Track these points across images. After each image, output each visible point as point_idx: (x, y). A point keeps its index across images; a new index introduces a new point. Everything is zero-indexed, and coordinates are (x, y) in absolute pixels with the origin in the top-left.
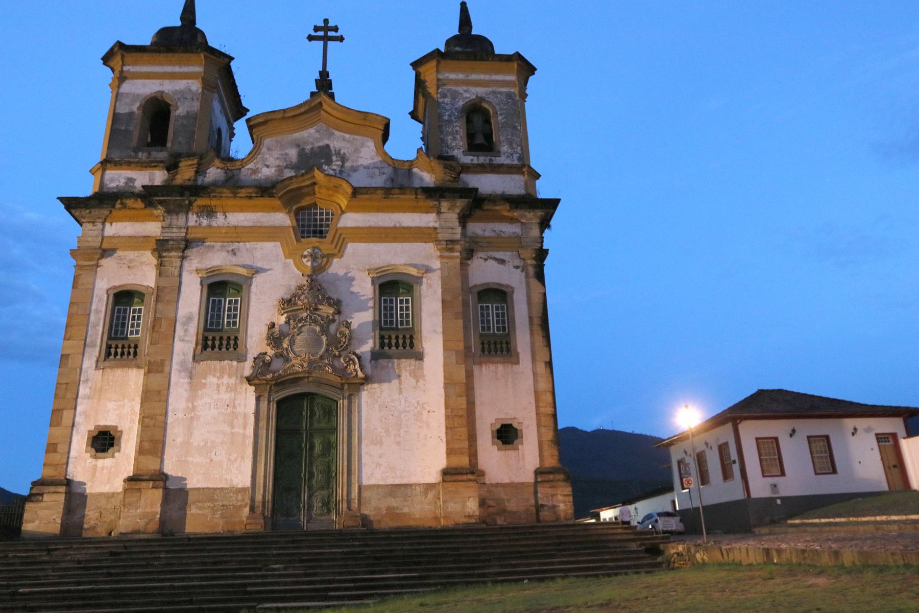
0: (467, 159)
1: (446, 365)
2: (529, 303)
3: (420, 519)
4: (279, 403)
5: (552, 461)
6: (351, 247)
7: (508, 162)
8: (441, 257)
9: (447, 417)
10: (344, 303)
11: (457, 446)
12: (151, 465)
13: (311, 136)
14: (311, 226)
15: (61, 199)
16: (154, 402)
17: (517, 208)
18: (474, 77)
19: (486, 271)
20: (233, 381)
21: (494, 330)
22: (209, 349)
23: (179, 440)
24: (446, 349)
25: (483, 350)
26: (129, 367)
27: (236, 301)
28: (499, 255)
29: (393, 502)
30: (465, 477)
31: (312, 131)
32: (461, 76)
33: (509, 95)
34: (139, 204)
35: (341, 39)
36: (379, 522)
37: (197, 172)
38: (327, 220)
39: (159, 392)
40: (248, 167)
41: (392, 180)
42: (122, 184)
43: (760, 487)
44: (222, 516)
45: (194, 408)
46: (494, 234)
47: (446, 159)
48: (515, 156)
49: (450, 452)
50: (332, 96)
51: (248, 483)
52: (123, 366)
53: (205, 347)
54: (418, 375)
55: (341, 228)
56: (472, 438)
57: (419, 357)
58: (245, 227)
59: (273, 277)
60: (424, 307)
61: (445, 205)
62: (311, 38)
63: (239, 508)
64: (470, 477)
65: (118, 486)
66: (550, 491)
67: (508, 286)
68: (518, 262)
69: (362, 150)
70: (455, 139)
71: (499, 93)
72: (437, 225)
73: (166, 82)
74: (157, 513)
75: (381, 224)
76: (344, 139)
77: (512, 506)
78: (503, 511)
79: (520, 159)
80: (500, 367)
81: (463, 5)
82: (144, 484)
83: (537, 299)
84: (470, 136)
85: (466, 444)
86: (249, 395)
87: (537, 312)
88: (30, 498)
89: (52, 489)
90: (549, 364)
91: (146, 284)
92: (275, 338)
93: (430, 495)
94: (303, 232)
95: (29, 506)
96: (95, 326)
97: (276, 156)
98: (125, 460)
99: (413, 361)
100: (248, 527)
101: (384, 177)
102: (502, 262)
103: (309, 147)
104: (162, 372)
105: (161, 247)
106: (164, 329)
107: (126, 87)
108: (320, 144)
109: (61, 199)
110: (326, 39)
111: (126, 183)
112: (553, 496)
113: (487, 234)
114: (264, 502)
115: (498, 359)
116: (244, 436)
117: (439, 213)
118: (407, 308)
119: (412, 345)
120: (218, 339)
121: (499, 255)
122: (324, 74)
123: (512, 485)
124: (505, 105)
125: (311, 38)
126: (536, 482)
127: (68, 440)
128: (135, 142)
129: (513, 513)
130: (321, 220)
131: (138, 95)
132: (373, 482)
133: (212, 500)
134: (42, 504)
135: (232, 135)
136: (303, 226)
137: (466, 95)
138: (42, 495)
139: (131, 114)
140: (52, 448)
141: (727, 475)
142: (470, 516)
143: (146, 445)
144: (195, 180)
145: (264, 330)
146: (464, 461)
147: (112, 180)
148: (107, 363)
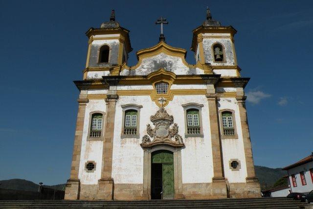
0: (213, 64)
3: (206, 196)
5: (253, 175)
7: (230, 65)
9: (213, 158)
11: (217, 169)
12: (107, 175)
15: (75, 82)
16: (108, 153)
19: (224, 105)
22: (126, 134)
24: (212, 133)
27: (135, 117)
30: (221, 181)
31: (159, 55)
33: (228, 41)
36: (190, 197)
39: (110, 149)
41: (188, 72)
42: (94, 77)
47: (208, 64)
49: (215, 171)
51: (142, 183)
53: (125, 133)
57: (202, 136)
59: (148, 107)
62: (156, 24)
64: (223, 180)
65: (96, 182)
67: (232, 110)
74: (110, 193)
76: (171, 58)
79: (234, 64)
80: (231, 140)
82: (106, 182)
84: (215, 56)
85: (221, 168)
86: (142, 151)
88: (67, 185)
89: (74, 182)
90: (250, 138)
92: (150, 130)
93: (208, 187)
94: (158, 91)
97: (148, 64)
100: (143, 198)
101: (186, 71)
102: (230, 101)
104: (110, 142)
105: (109, 98)
106: (110, 127)
108: (163, 60)
109: (75, 82)
112: (253, 187)
114: (148, 189)
115: (231, 137)
118: (197, 119)
120: (130, 131)
121: (229, 99)
127: (220, 160)
128: (97, 61)
130: (164, 87)
133: (129, 188)
134: (70, 188)
135: (128, 58)
136: (158, 89)
143: (106, 168)
144: (119, 74)
145: (146, 128)
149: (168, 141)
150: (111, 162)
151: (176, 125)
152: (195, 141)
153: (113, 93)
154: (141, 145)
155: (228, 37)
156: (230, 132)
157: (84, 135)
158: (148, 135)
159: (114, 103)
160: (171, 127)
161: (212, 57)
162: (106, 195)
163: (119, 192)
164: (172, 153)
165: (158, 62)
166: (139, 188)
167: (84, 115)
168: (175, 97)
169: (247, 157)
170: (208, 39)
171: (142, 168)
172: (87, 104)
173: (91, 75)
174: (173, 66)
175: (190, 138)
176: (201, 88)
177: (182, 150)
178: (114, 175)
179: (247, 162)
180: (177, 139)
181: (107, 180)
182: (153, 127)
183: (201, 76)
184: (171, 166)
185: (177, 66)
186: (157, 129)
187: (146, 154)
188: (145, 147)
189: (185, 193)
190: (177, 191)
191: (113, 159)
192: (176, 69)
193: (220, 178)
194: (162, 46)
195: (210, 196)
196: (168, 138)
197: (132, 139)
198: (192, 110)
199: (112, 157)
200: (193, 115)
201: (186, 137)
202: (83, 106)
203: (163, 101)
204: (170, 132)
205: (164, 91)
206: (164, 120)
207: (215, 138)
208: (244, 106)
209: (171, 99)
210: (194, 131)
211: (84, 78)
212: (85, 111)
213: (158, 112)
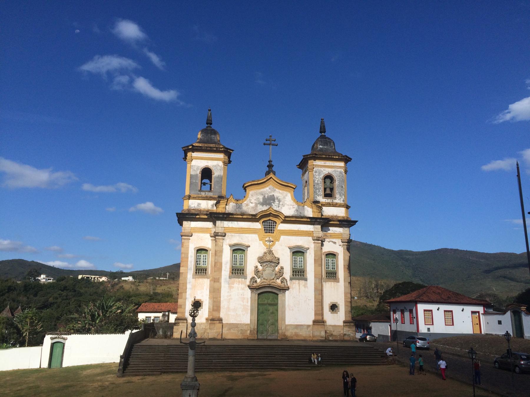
1: (315, 284)
4: (259, 294)
5: (349, 319)
12: (215, 315)
14: (269, 228)
19: (328, 247)
20: (243, 286)
21: (330, 269)
23: (226, 306)
24: (315, 277)
28: (334, 240)
29: (296, 330)
31: (267, 188)
33: (341, 173)
37: (226, 205)
40: (245, 202)
42: (196, 206)
44: (241, 333)
45: (230, 295)
46: (332, 232)
47: (316, 202)
48: (342, 199)
49: (316, 314)
51: (249, 322)
54: (305, 286)
57: (306, 280)
59: (256, 248)
62: (264, 144)
63: (246, 331)
64: (322, 323)
70: (319, 191)
71: (337, 171)
73: (209, 161)
76: (279, 193)
77: (334, 333)
78: (332, 335)
79: (343, 201)
80: (332, 283)
81: (322, 123)
82: (215, 322)
84: (325, 189)
89: (182, 321)
91: (208, 246)
92: (257, 272)
94: (265, 230)
95: (175, 327)
96: (191, 262)
101: (294, 209)
102: (335, 243)
103: (266, 196)
105: (215, 235)
106: (218, 266)
107: (194, 163)
120: (238, 271)
121: (334, 240)
123: (335, 326)
126: (344, 326)
129: (335, 336)
131: (198, 167)
132: (290, 323)
133: (237, 327)
137: (324, 172)
139: (197, 175)
141: (412, 323)
143: (215, 308)
145: (253, 269)
146: (320, 318)
147: (192, 204)
148: (196, 276)
149: (274, 284)
150: (220, 302)
151: (282, 268)
152: (299, 283)
153: (220, 230)
154: (249, 286)
155: (340, 167)
156: (332, 275)
157: (189, 271)
159: (221, 241)
160: (277, 269)
161: (322, 192)
162: (216, 335)
163: (227, 332)
164: (278, 295)
166: (245, 328)
167: (188, 250)
168: (282, 238)
169: (346, 301)
170: (320, 169)
171: (250, 308)
172: (190, 238)
173: (193, 204)
174: (281, 203)
178: (222, 315)
179: (345, 305)
180: (282, 282)
181: (215, 320)
182: (260, 268)
183: (310, 218)
184: (276, 307)
185: (286, 202)
186: (264, 270)
189: (288, 334)
190: (280, 331)
191: (222, 299)
193: (319, 322)
194: (271, 177)
195: (310, 337)
196: (274, 280)
200: (299, 258)
201: (291, 279)
202: (186, 241)
203: (270, 241)
204: (276, 275)
205: (271, 230)
206: (271, 262)
208: (348, 249)
209: (278, 240)
210: (299, 273)
211: (185, 207)
212: (189, 246)
213: (265, 253)
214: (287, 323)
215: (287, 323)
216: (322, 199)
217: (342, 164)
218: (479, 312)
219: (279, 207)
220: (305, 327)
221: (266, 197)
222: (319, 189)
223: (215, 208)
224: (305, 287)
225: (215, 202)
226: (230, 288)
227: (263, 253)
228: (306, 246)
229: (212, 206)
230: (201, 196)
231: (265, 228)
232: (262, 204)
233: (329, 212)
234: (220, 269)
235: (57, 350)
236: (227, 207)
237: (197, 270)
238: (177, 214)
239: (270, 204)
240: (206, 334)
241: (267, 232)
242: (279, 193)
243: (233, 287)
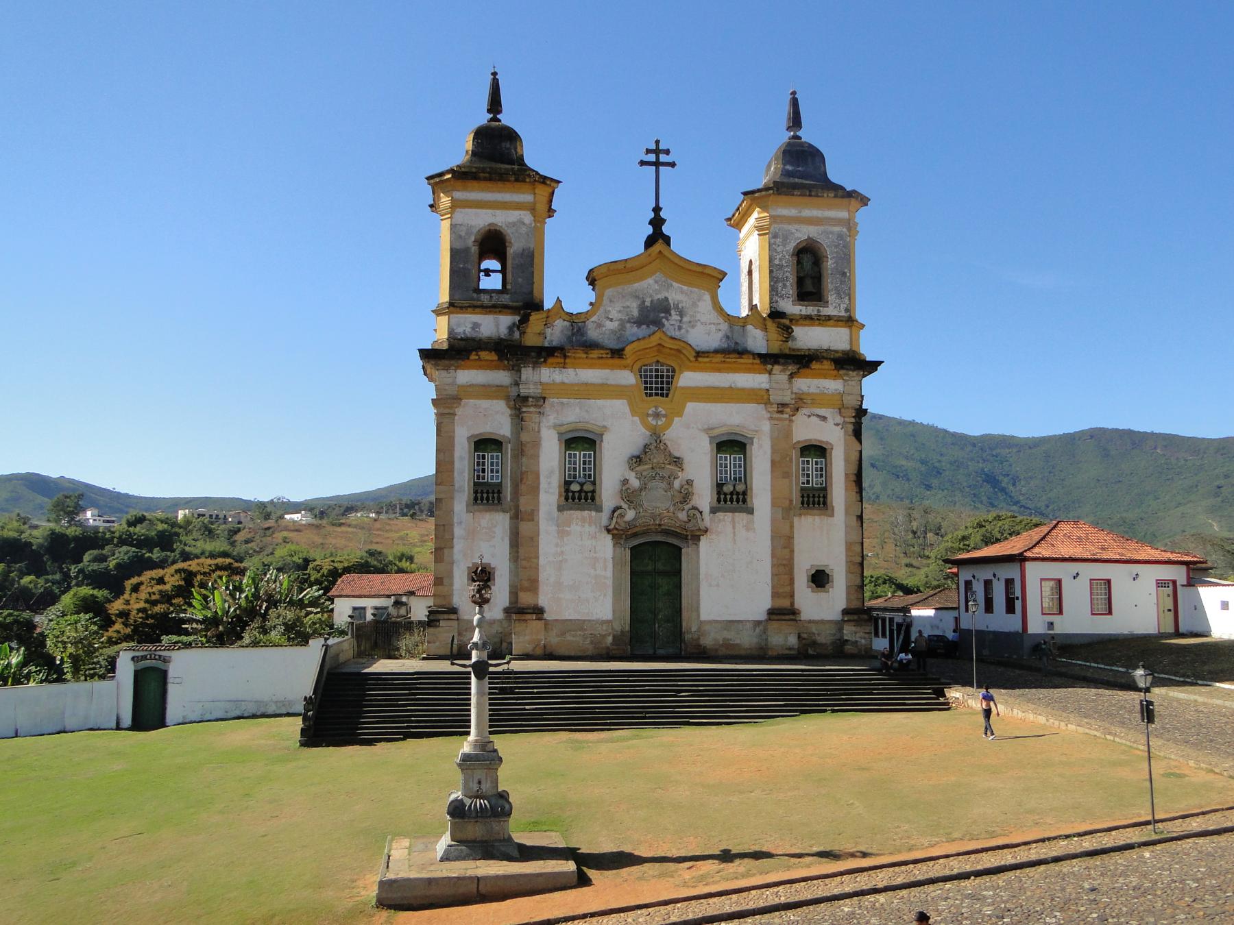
1: (774, 521)
2: (847, 460)
6: (690, 407)
8: (771, 418)
9: (773, 566)
10: (685, 461)
13: (651, 286)
17: (842, 368)
18: (807, 213)
19: (807, 429)
20: (593, 529)
24: (774, 504)
25: (802, 503)
26: (497, 511)
27: (590, 456)
28: (822, 412)
31: (650, 281)
32: (793, 212)
33: (840, 236)
34: (493, 356)
35: (673, 165)
38: (668, 377)
39: (532, 539)
41: (728, 337)
42: (468, 330)
43: (1036, 626)
44: (592, 642)
46: (818, 391)
48: (843, 306)
49: (775, 595)
50: (667, 240)
52: (490, 511)
53: (567, 499)
55: (683, 388)
56: (792, 581)
57: (750, 511)
58: (593, 384)
59: (622, 432)
60: (754, 465)
61: (776, 367)
62: (642, 163)
63: (604, 636)
66: (854, 629)
67: (827, 443)
68: (839, 419)
69: (700, 304)
70: (785, 286)
71: (832, 233)
72: (767, 386)
73: (498, 212)
75: (717, 384)
76: (682, 292)
77: (820, 639)
79: (847, 310)
81: (795, 103)
82: (528, 617)
83: (855, 456)
84: (800, 282)
87: (854, 469)
89: (446, 616)
93: (758, 630)
94: (646, 388)
98: (500, 594)
99: (744, 516)
101: (720, 334)
102: (824, 418)
105: (520, 404)
108: (661, 296)
109: (421, 351)
110: (657, 164)
111: (473, 328)
113: (813, 390)
115: (815, 511)
116: (606, 578)
117: (770, 373)
119: (744, 501)
120: (578, 494)
122: (657, 209)
123: (822, 622)
124: (836, 247)
125: (642, 163)
126: (843, 620)
131: (470, 228)
133: (582, 629)
137: (798, 235)
138: (438, 621)
140: (438, 581)
141: (1010, 609)
142: (790, 649)
145: (618, 486)
146: (785, 603)
147: (459, 325)
150: (537, 568)
151: (690, 483)
152: (733, 519)
155: (839, 222)
157: (457, 495)
158: (625, 506)
159: (535, 417)
161: (790, 289)
164: (680, 549)
165: (648, 304)
166: (603, 630)
168: (690, 407)
169: (849, 563)
170: (786, 227)
171: (610, 582)
174: (685, 319)
175: (720, 515)
176: (756, 386)
177: (704, 541)
178: (543, 600)
179: (849, 572)
182: (635, 483)
183: (760, 356)
185: (698, 317)
187: (618, 550)
188: (618, 534)
190: (687, 637)
191: (542, 561)
192: (693, 327)
193: (783, 613)
197: (586, 513)
198: (731, 445)
199: (537, 557)
200: (731, 459)
201: (714, 511)
203: (657, 415)
207: (780, 516)
210: (732, 497)
213: (646, 446)
214: (704, 616)
215: (704, 616)
216: (791, 307)
217: (843, 214)
218: (1174, 582)
219: (680, 328)
220: (748, 625)
221: (648, 304)
222: (784, 280)
223: (517, 335)
224: (748, 529)
225: (517, 318)
226: (562, 534)
227: (641, 446)
228: (753, 427)
229: (511, 329)
230: (479, 303)
231: (646, 382)
232: (639, 323)
233: (809, 337)
234: (535, 490)
235: (152, 686)
236: (548, 331)
237: (476, 492)
238: (421, 351)
239: (658, 324)
240: (504, 645)
241: (651, 395)
242: (677, 294)
243: (568, 533)
